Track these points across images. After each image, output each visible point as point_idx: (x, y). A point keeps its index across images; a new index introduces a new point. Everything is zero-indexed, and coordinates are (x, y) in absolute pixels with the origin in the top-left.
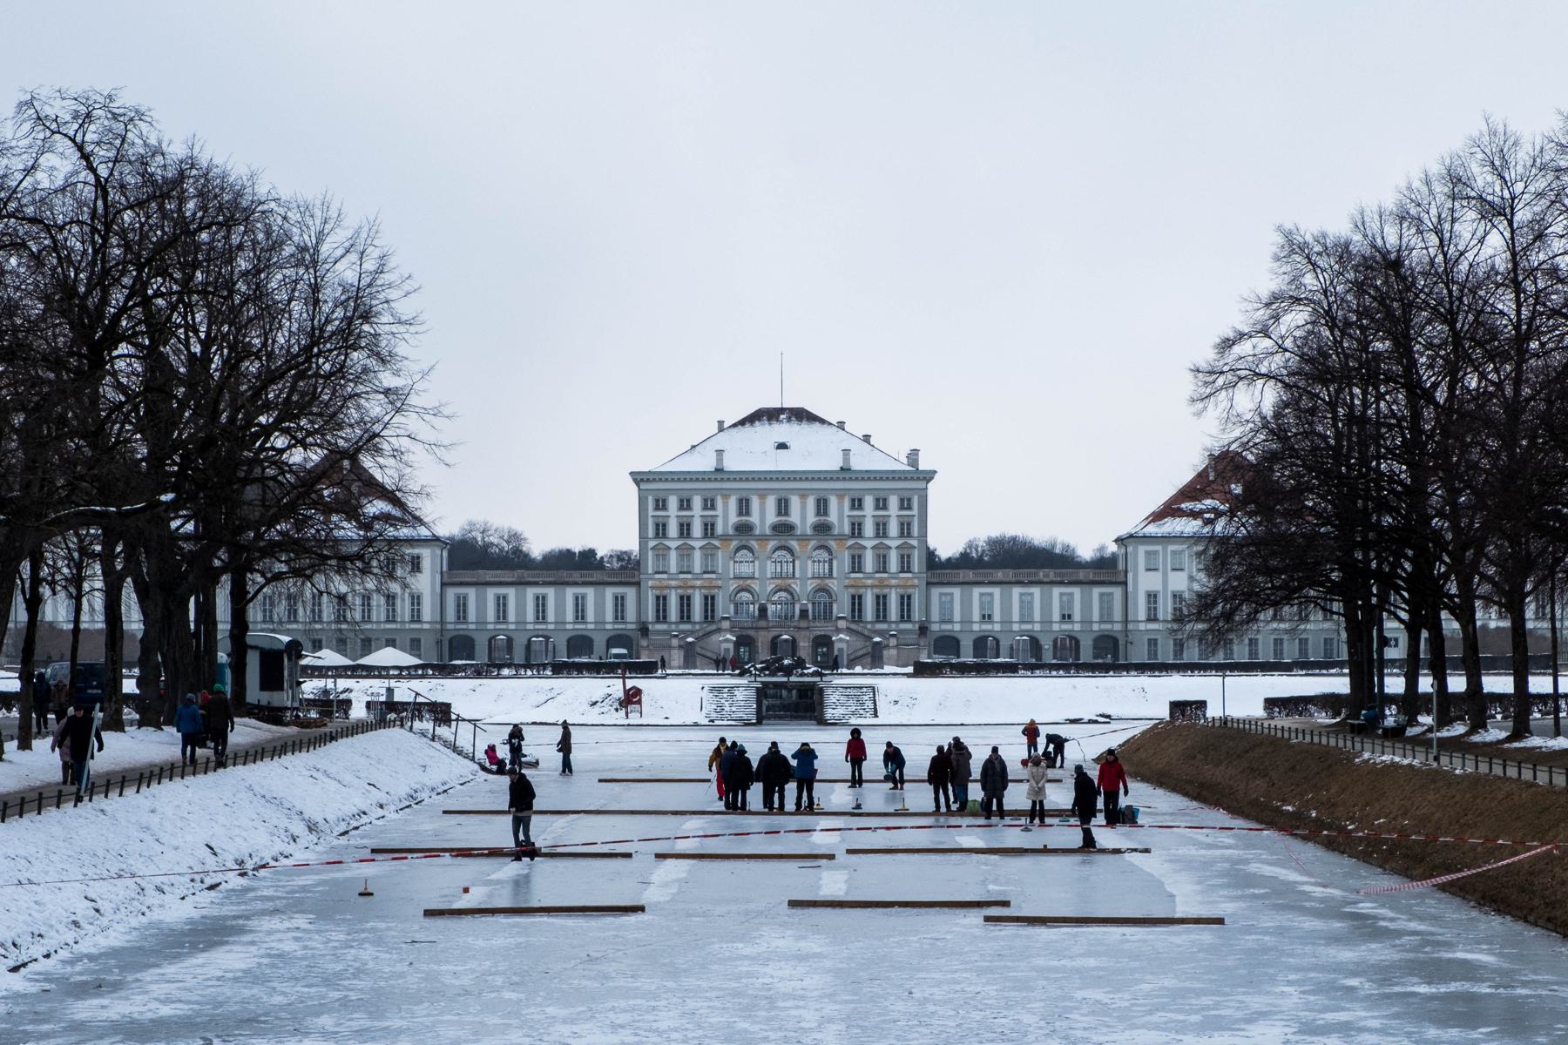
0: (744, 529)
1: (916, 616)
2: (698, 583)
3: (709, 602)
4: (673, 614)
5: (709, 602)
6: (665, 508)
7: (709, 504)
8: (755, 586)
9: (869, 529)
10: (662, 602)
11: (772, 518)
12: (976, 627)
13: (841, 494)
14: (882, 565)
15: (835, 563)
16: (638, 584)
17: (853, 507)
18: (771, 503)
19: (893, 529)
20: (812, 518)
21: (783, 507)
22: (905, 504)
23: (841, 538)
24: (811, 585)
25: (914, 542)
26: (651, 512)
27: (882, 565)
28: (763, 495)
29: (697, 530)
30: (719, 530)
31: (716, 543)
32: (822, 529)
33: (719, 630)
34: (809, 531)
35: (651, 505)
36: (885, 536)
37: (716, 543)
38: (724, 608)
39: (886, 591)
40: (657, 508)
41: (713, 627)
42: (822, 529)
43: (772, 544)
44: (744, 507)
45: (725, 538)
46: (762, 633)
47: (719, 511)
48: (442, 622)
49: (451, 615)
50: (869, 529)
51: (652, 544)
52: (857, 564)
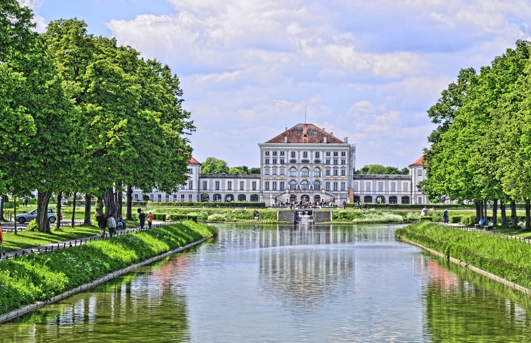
1: (346, 189)
2: (279, 178)
3: (282, 184)
5: (282, 184)
7: (282, 154)
8: (297, 179)
9: (332, 162)
10: (267, 184)
11: (302, 158)
13: (323, 151)
14: (336, 173)
16: (260, 178)
17: (327, 155)
18: (302, 153)
19: (340, 162)
20: (314, 159)
21: (305, 155)
22: (343, 154)
23: (323, 164)
24: (314, 179)
25: (346, 166)
26: (264, 156)
27: (336, 173)
28: (299, 151)
29: (278, 162)
30: (285, 162)
31: (285, 166)
32: (317, 162)
33: (285, 193)
34: (313, 162)
36: (337, 164)
38: (286, 186)
39: (337, 181)
41: (283, 192)
42: (317, 162)
43: (302, 166)
44: (293, 155)
46: (298, 194)
47: (285, 156)
48: (199, 190)
49: (202, 187)
50: (332, 162)
51: (264, 166)
52: (328, 173)
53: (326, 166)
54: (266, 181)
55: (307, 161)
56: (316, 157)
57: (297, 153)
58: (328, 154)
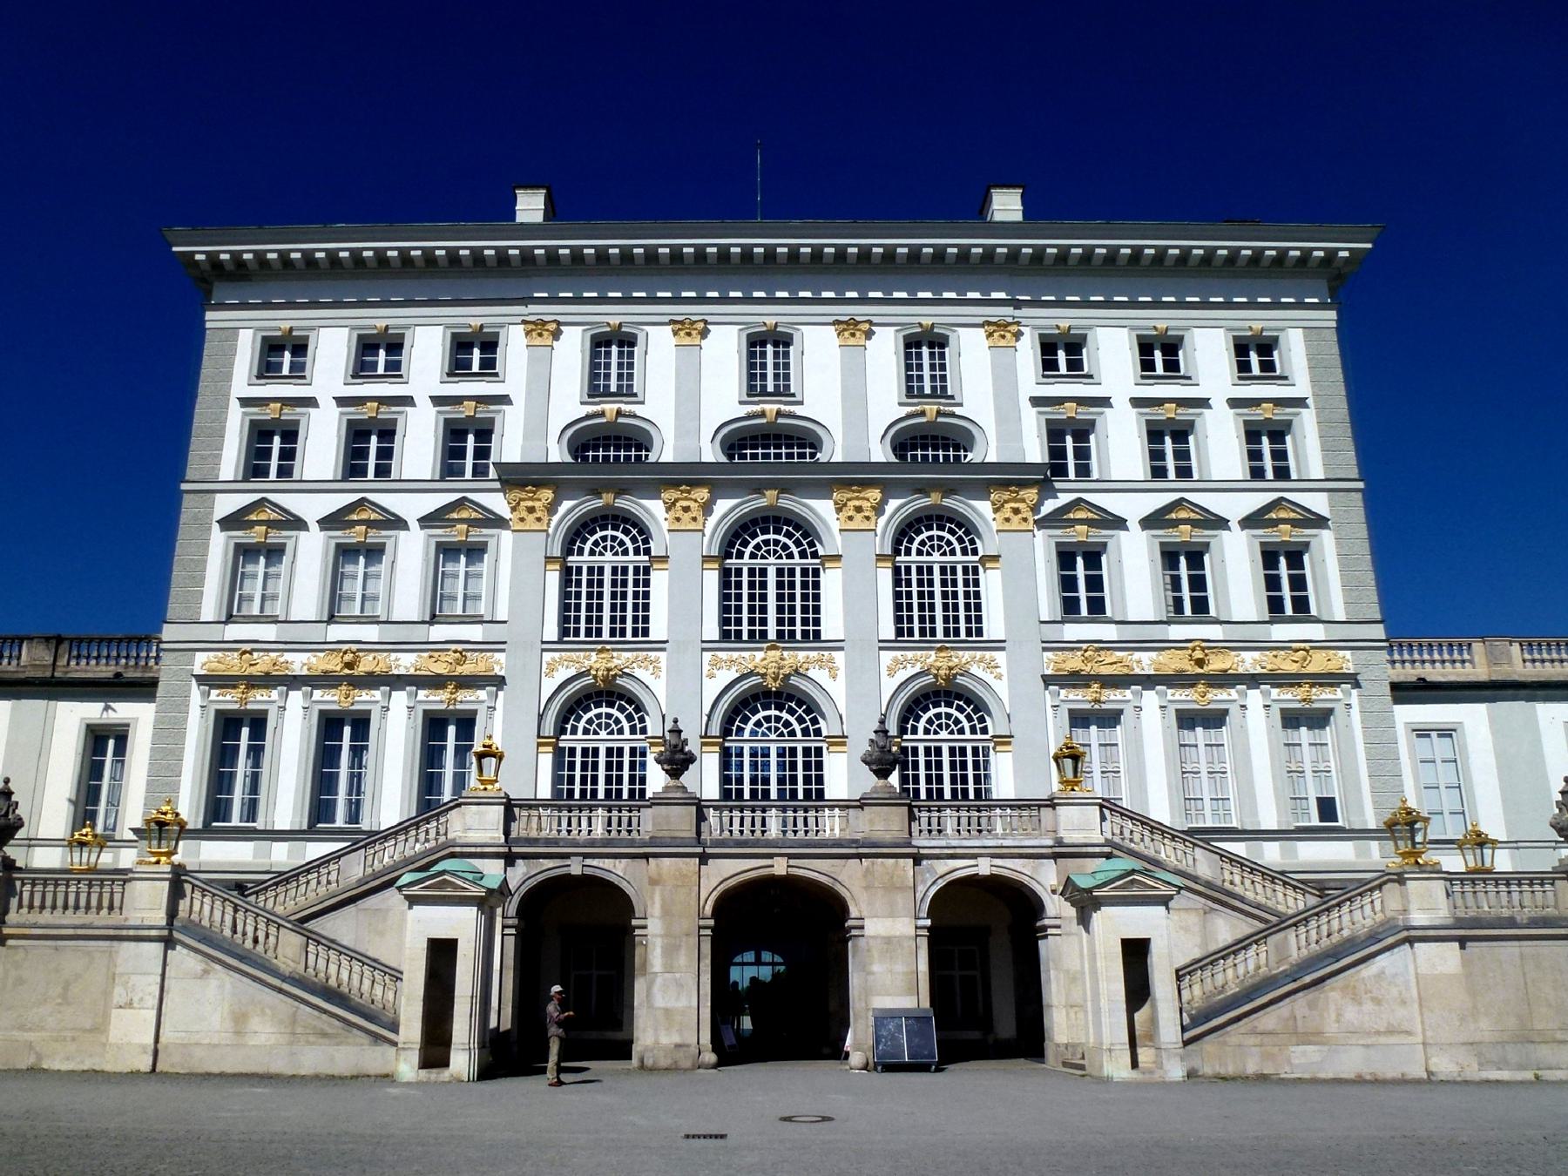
2: (405, 663)
7: (472, 352)
9: (1121, 446)
10: (237, 733)
15: (991, 583)
17: (1049, 365)
18: (724, 348)
19: (1220, 446)
22: (1254, 353)
24: (894, 673)
26: (242, 381)
35: (246, 349)
37: (497, 503)
40: (267, 369)
50: (1121, 446)
51: (227, 504)
54: (229, 699)
55: (804, 439)
56: (912, 390)
57: (659, 348)
58: (1063, 352)
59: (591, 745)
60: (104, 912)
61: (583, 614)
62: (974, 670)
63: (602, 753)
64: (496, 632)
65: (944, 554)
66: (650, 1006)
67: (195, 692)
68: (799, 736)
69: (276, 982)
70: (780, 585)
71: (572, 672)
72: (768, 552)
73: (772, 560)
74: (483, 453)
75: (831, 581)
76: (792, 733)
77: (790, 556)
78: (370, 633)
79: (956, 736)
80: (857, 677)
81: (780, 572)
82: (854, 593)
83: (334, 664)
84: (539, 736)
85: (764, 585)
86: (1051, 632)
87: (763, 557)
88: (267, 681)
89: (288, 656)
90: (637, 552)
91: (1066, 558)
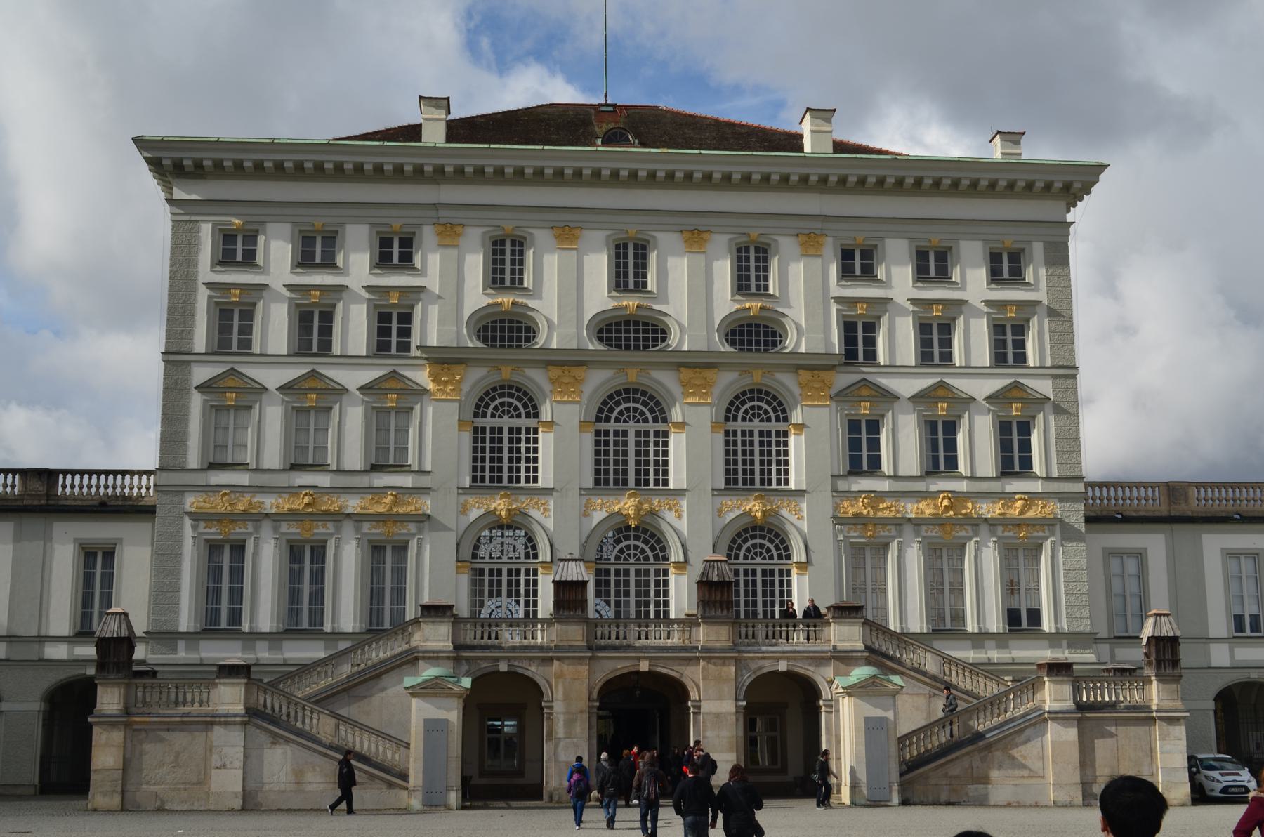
0: (505, 330)
2: (353, 504)
4: (264, 611)
5: (386, 555)
6: (249, 260)
9: (898, 341)
11: (599, 296)
12: (1220, 656)
19: (973, 341)
25: (1044, 387)
26: (205, 270)
33: (412, 659)
40: (225, 259)
41: (396, 647)
42: (754, 334)
45: (443, 360)
51: (201, 374)
53: (844, 379)
54: (213, 532)
58: (858, 262)
59: (495, 567)
60: (197, 704)
61: (488, 464)
62: (784, 512)
63: (505, 573)
64: (424, 481)
65: (762, 420)
66: (556, 761)
67: (188, 523)
68: (652, 560)
69: (324, 750)
70: (638, 444)
71: (482, 511)
72: (629, 417)
73: (631, 423)
74: (405, 332)
75: (677, 445)
76: (646, 558)
77: (646, 421)
78: (324, 480)
79: (768, 561)
80: (692, 514)
81: (638, 433)
82: (690, 452)
83: (299, 503)
84: (458, 561)
85: (625, 444)
86: (842, 485)
87: (625, 421)
88: (246, 516)
89: (257, 499)
90: (528, 416)
91: (853, 426)
